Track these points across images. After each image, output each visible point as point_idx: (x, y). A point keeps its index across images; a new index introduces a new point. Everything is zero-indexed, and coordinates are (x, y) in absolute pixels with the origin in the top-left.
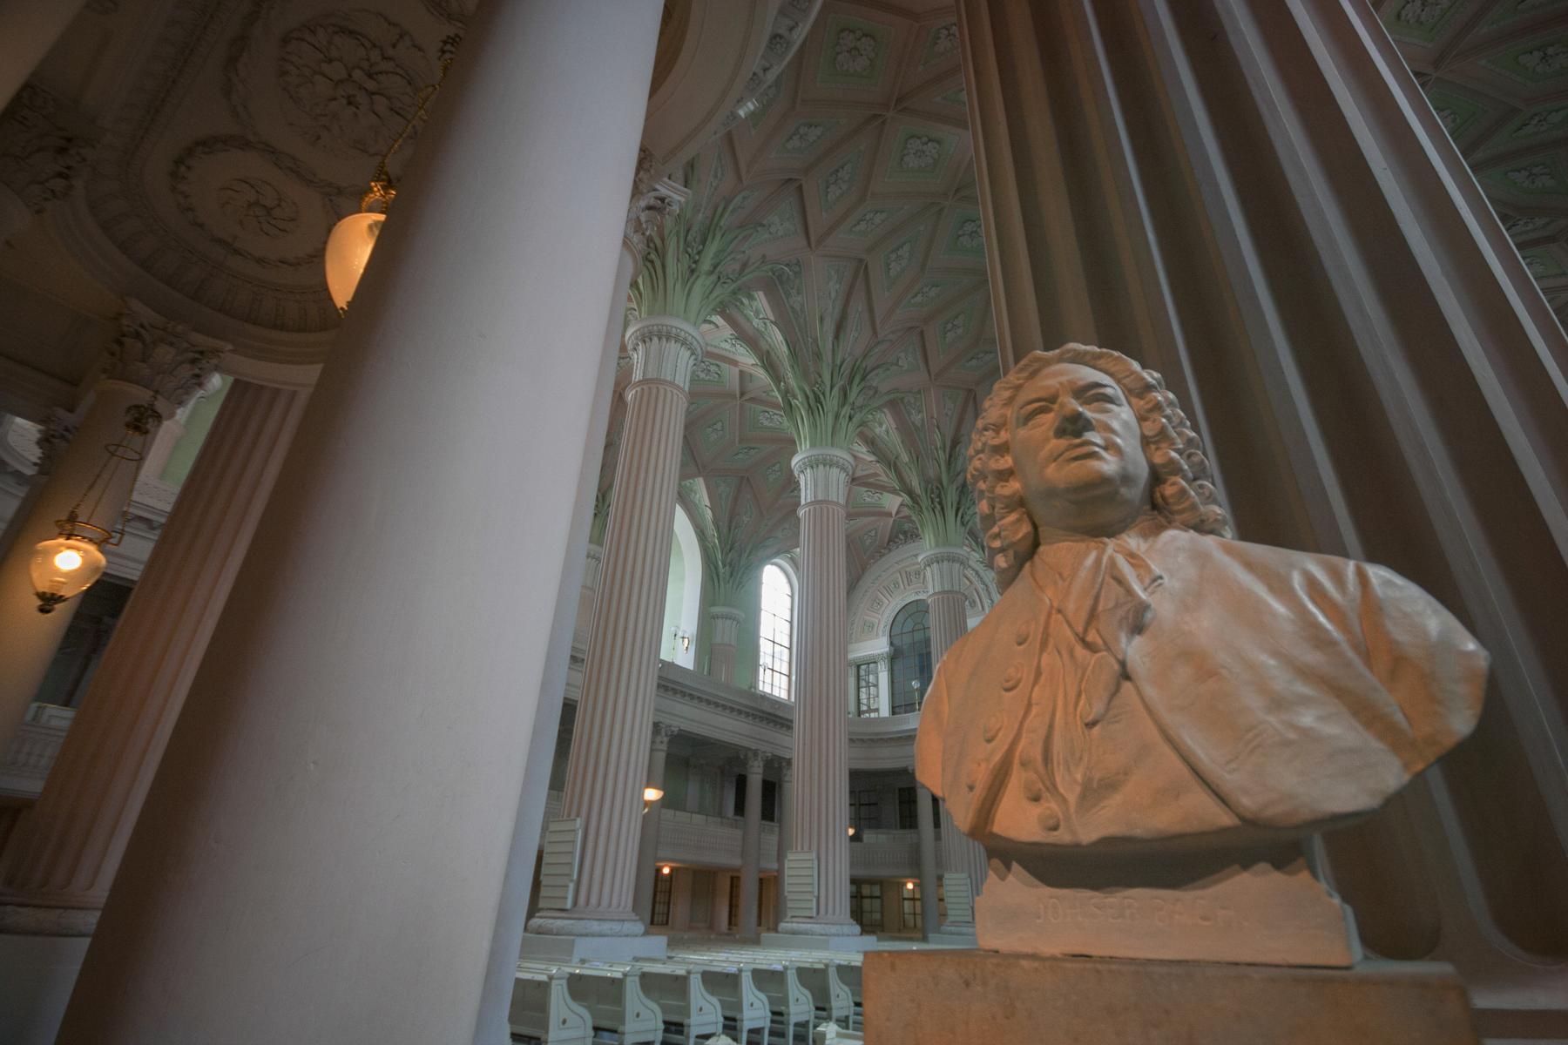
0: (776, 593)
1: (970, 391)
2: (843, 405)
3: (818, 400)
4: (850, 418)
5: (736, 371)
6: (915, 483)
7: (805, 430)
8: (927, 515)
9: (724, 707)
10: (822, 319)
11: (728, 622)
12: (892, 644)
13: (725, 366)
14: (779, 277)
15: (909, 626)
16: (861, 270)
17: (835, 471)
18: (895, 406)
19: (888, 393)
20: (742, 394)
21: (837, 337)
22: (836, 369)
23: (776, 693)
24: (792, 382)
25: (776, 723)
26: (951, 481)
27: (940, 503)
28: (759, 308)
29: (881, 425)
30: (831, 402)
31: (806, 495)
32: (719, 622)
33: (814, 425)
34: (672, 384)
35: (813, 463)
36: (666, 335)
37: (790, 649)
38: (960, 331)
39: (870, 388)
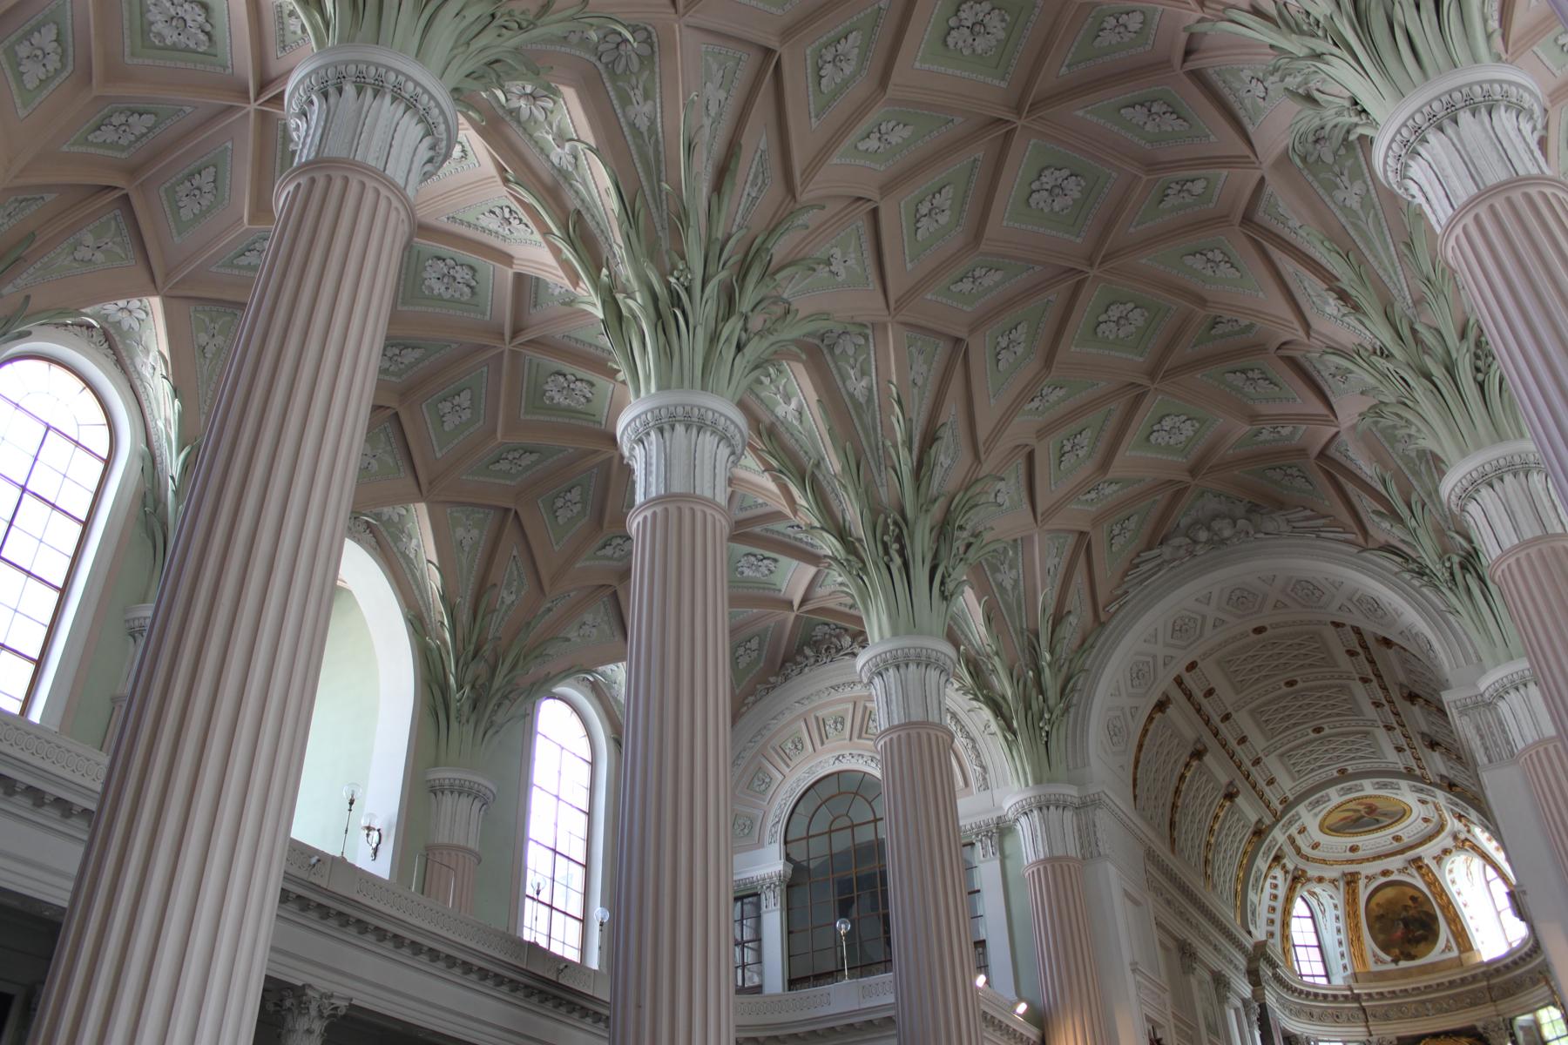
0: (563, 754)
1: (958, 341)
2: (727, 318)
3: (676, 301)
4: (739, 348)
5: (510, 272)
6: (852, 512)
7: (647, 362)
8: (875, 576)
9: (451, 962)
10: (690, 148)
11: (464, 802)
12: (788, 858)
13: (486, 265)
14: (611, 67)
15: (820, 825)
16: (769, 63)
17: (708, 441)
18: (818, 354)
19: (811, 317)
20: (516, 332)
21: (718, 187)
22: (714, 250)
23: (556, 949)
24: (626, 272)
25: (559, 1002)
26: (923, 508)
27: (901, 552)
28: (565, 122)
29: (787, 399)
30: (704, 309)
31: (645, 484)
32: (448, 800)
33: (667, 353)
34: (380, 175)
35: (663, 423)
36: (372, 84)
37: (587, 867)
38: (943, 219)
39: (777, 300)
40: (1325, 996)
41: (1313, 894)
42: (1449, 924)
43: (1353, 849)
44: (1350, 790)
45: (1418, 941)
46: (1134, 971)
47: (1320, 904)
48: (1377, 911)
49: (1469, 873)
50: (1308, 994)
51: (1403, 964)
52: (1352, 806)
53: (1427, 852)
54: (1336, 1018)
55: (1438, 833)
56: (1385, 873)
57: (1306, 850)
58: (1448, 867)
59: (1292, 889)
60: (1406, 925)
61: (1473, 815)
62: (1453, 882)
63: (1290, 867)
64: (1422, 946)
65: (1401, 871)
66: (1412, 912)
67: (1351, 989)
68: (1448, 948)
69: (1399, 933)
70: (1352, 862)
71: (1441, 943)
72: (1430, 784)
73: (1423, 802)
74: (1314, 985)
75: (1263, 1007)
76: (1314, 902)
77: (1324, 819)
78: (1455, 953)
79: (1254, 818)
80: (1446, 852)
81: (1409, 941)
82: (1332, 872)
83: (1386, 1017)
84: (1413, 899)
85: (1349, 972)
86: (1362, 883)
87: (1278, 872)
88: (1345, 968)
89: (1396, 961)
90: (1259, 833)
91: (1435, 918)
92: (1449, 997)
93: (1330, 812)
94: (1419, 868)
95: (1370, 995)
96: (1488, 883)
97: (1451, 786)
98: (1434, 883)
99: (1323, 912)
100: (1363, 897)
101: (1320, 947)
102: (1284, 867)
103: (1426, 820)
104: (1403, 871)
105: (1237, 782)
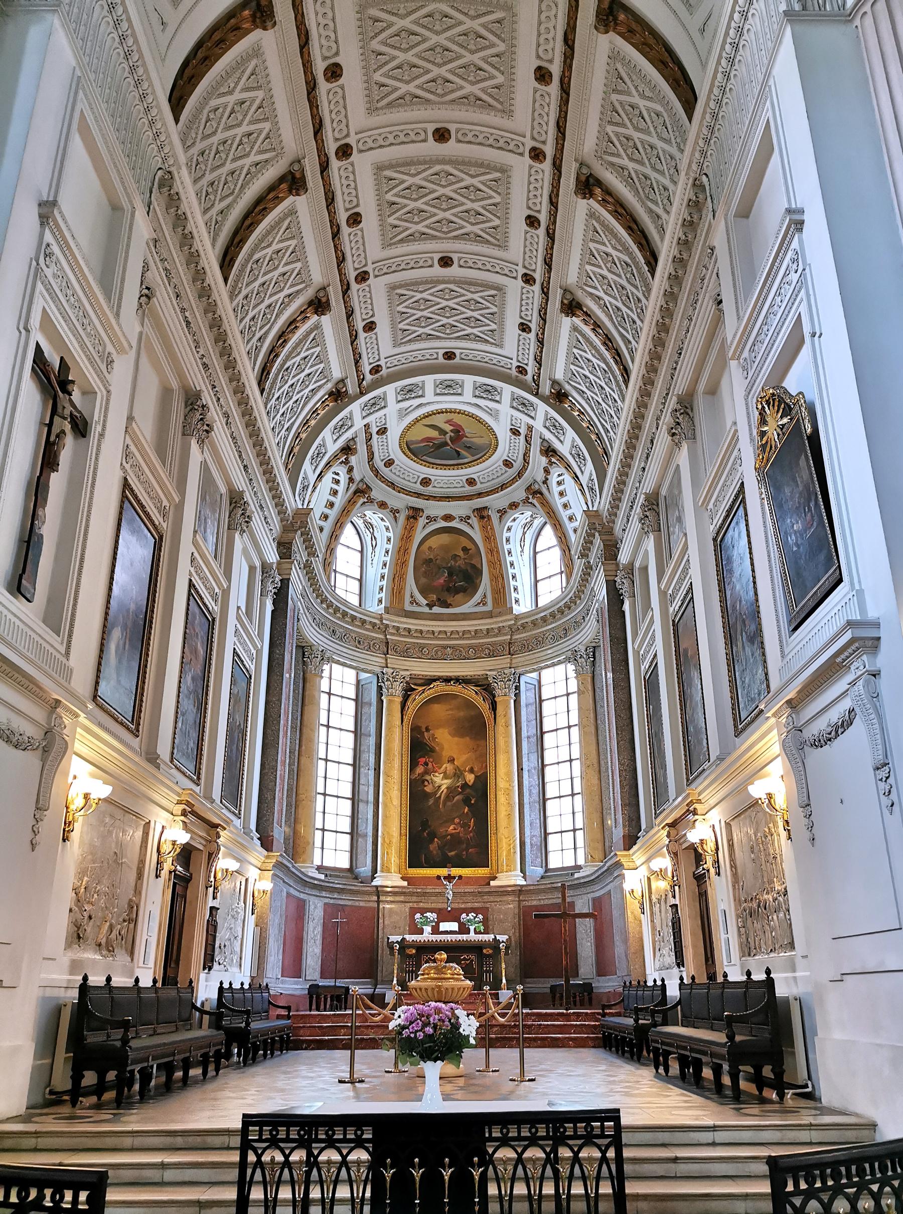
40: (354, 618)
41: (369, 526)
42: (491, 580)
43: (426, 482)
44: (449, 388)
45: (457, 591)
46: (45, 219)
47: (373, 537)
48: (428, 555)
49: (523, 540)
50: (337, 610)
51: (436, 610)
52: (439, 421)
53: (496, 501)
54: (359, 642)
55: (514, 481)
56: (448, 518)
57: (379, 463)
58: (509, 524)
59: (351, 502)
60: (450, 574)
61: (568, 442)
62: (508, 540)
63: (357, 476)
64: (459, 597)
65: (462, 519)
66: (460, 563)
67: (381, 619)
68: (483, 602)
69: (442, 581)
70: (419, 495)
71: (477, 597)
72: (537, 395)
73: (515, 432)
74: (345, 603)
75: (285, 582)
76: (368, 538)
77: (409, 428)
78: (489, 607)
79: (337, 374)
80: (514, 506)
81: (448, 590)
82: (399, 501)
83: (405, 653)
84: (465, 549)
85: (383, 605)
86: (422, 521)
87: (343, 478)
88: (380, 601)
89: (430, 606)
90: (338, 396)
91: (480, 572)
92: (471, 647)
93: (417, 421)
94: (482, 517)
95: (398, 629)
96: (535, 553)
97: (559, 397)
98: (490, 537)
99: (374, 547)
100: (419, 535)
101: (360, 581)
102: (350, 470)
103: (507, 464)
104: (465, 519)
105: (330, 290)
